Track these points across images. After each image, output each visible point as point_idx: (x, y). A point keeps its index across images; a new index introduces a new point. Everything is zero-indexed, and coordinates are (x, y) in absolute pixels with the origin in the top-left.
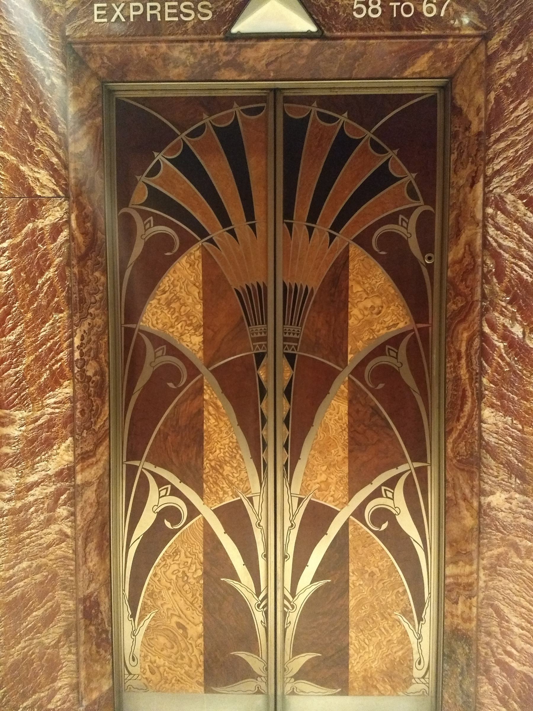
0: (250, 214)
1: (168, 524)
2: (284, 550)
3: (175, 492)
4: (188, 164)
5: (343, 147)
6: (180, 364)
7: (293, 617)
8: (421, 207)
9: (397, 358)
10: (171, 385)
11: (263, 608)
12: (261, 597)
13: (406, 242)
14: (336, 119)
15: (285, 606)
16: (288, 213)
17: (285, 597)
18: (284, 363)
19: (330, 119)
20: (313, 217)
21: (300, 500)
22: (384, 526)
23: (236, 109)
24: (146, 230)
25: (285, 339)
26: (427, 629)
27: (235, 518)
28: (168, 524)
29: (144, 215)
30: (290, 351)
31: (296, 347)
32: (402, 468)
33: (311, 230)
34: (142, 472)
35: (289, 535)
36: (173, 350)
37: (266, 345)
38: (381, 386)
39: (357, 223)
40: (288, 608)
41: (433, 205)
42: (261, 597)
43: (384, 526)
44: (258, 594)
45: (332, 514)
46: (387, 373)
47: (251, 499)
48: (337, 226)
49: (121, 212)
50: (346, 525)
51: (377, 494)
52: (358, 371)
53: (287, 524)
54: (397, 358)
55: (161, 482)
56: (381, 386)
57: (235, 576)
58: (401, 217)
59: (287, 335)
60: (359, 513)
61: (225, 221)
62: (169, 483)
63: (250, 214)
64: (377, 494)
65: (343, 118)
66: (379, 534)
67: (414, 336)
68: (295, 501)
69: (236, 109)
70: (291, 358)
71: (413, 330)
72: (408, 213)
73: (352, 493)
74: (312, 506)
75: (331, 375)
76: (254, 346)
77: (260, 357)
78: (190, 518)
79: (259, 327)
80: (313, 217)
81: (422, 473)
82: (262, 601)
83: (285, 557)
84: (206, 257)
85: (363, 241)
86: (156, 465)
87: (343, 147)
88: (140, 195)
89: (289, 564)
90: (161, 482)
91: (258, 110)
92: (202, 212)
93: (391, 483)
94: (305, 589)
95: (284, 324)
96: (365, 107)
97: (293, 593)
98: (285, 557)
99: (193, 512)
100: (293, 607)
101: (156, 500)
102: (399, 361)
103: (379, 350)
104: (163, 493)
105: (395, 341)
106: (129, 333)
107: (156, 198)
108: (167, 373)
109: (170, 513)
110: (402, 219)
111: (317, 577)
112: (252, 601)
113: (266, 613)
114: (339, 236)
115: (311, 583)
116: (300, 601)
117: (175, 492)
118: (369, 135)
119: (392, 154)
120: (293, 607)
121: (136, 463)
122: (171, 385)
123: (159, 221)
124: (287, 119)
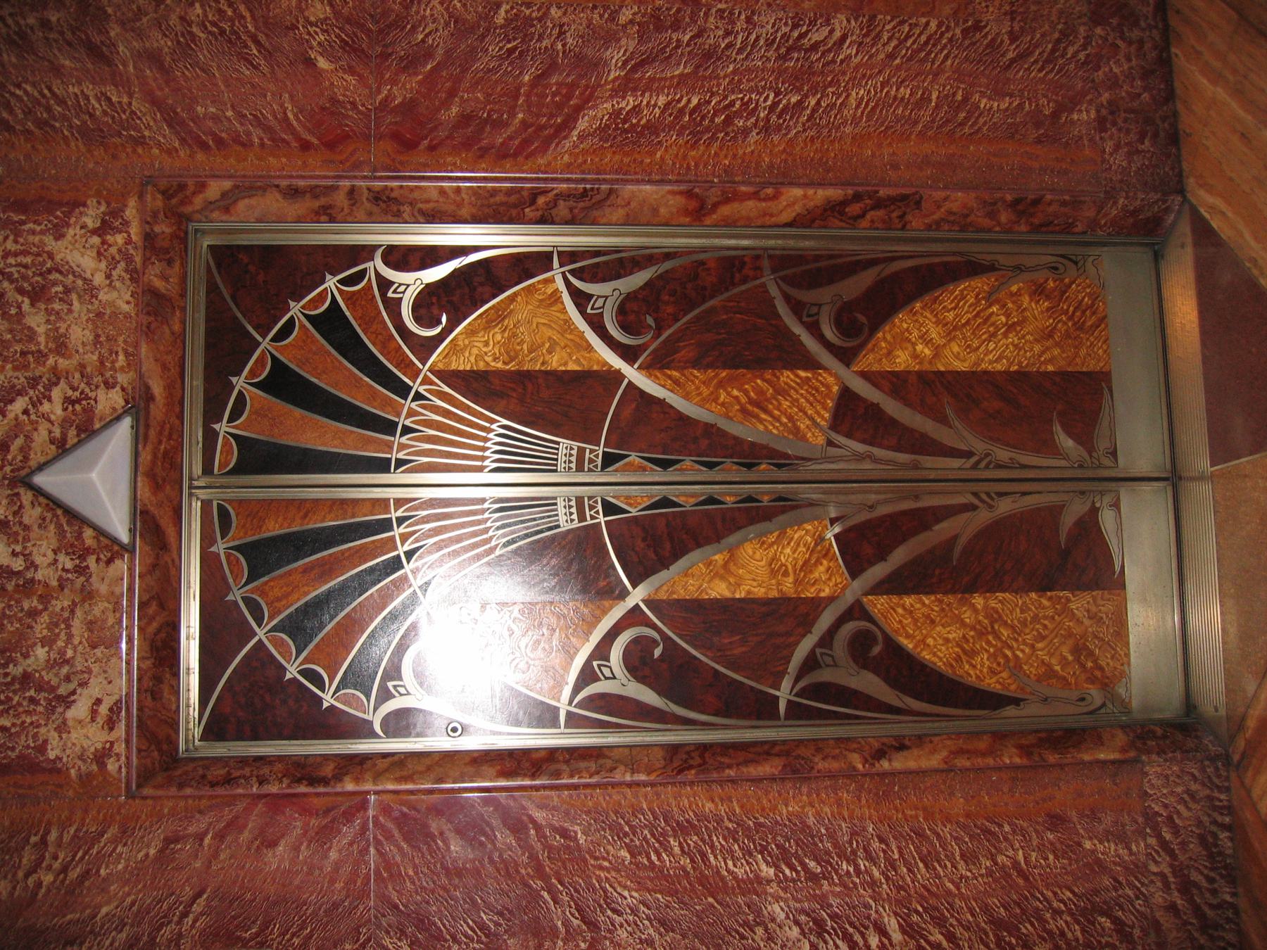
1: (876, 650)
2: (904, 466)
3: (827, 640)
5: (283, 383)
8: (378, 264)
9: (607, 297)
10: (657, 652)
11: (992, 499)
12: (976, 502)
14: (240, 393)
15: (987, 467)
17: (975, 467)
22: (862, 318)
23: (220, 547)
25: (580, 468)
28: (876, 650)
31: (592, 451)
32: (774, 291)
33: (407, 430)
34: (796, 695)
37: (590, 498)
40: (990, 463)
41: (374, 248)
42: (976, 502)
43: (862, 318)
44: (973, 508)
50: (864, 375)
52: (628, 354)
53: (867, 465)
54: (607, 297)
55: (811, 664)
58: (390, 294)
59: (573, 466)
60: (846, 356)
62: (813, 651)
64: (814, 329)
66: (874, 329)
67: (572, 272)
68: (832, 451)
69: (220, 547)
71: (563, 273)
72: (385, 284)
76: (592, 518)
79: (561, 510)
82: (983, 501)
87: (283, 383)
91: (224, 515)
93: (797, 308)
95: (556, 471)
96: (226, 350)
97: (968, 454)
99: (856, 611)
100: (987, 455)
109: (860, 647)
110: (395, 292)
111: (943, 420)
112: (983, 517)
113: (1000, 494)
115: (951, 427)
118: (265, 344)
119: (295, 309)
120: (987, 455)
121: (782, 706)
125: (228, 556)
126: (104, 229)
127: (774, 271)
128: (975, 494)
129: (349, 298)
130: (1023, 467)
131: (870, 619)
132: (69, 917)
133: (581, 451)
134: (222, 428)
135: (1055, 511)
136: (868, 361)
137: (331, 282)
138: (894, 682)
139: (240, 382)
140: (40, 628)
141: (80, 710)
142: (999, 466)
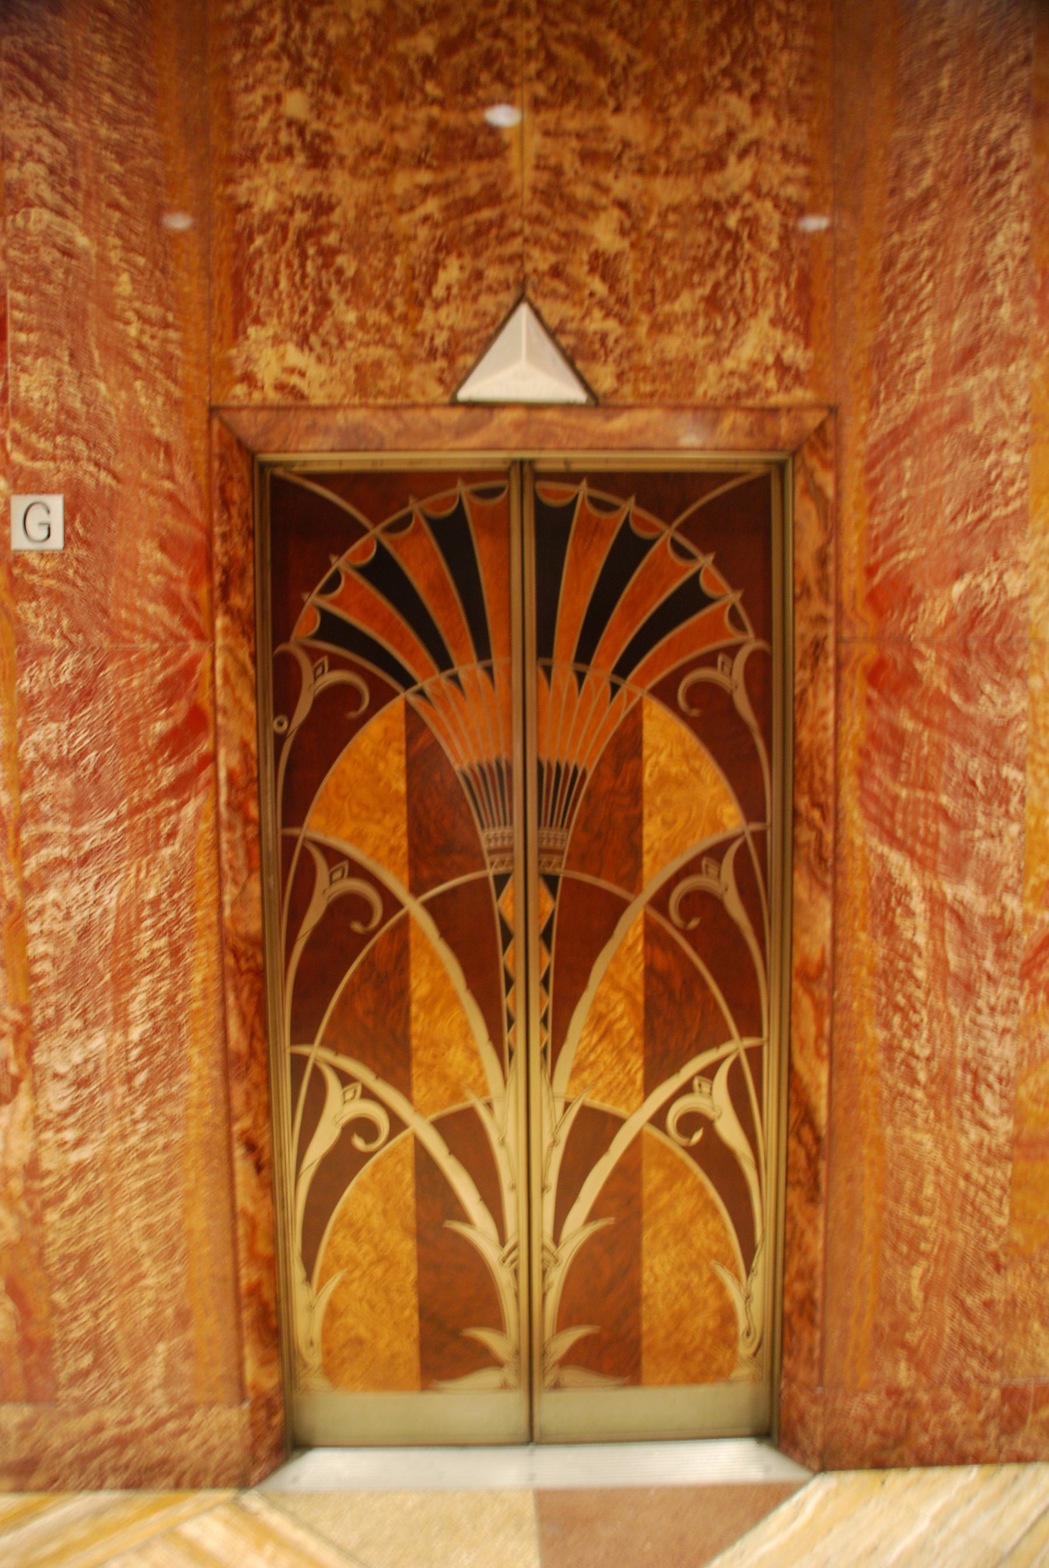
2: (543, 1177)
4: (384, 573)
5: (628, 551)
7: (557, 1277)
8: (751, 643)
10: (357, 927)
13: (729, 699)
16: (545, 647)
17: (543, 1248)
18: (539, 889)
19: (609, 508)
20: (585, 653)
21: (567, 1105)
22: (697, 1137)
23: (462, 489)
25: (541, 851)
26: (759, 1284)
27: (465, 1132)
29: (314, 655)
30: (549, 870)
32: (725, 1049)
35: (549, 1156)
36: (357, 870)
38: (694, 923)
43: (697, 1137)
44: (503, 1242)
45: (618, 1122)
46: (702, 903)
47: (489, 1105)
48: (623, 669)
49: (279, 649)
51: (687, 1089)
52: (659, 902)
53: (547, 1140)
55: (346, 1079)
56: (694, 923)
57: (466, 1219)
60: (658, 1119)
64: (687, 1089)
68: (560, 1106)
69: (462, 489)
70: (551, 881)
71: (742, 834)
72: (732, 651)
73: (648, 1089)
74: (586, 1111)
77: (501, 880)
78: (393, 1132)
79: (499, 831)
80: (585, 653)
81: (755, 1055)
83: (543, 1189)
84: (413, 720)
85: (665, 693)
86: (337, 1051)
87: (628, 551)
89: (550, 1197)
90: (346, 1079)
91: (494, 492)
93: (709, 1072)
94: (575, 1234)
96: (662, 489)
97: (556, 1239)
98: (543, 1189)
99: (397, 1124)
101: (340, 1108)
102: (723, 882)
103: (691, 868)
104: (349, 1095)
105: (717, 852)
106: (289, 843)
107: (333, 628)
108: (348, 907)
111: (593, 1216)
113: (516, 1272)
114: (627, 685)
116: (567, 1252)
117: (368, 1094)
118: (669, 533)
119: (705, 561)
120: (556, 1261)
122: (357, 927)
123: (336, 664)
125: (453, 498)
126: (781, 367)
127: (749, 1051)
128: (515, 1247)
129: (717, 615)
130: (544, 1295)
131: (391, 1136)
132: (96, 354)
133: (561, 853)
134: (583, 489)
135: (498, 1324)
137: (733, 597)
138: (327, 1162)
139: (629, 506)
140: (376, 316)
141: (294, 356)
142: (544, 1272)
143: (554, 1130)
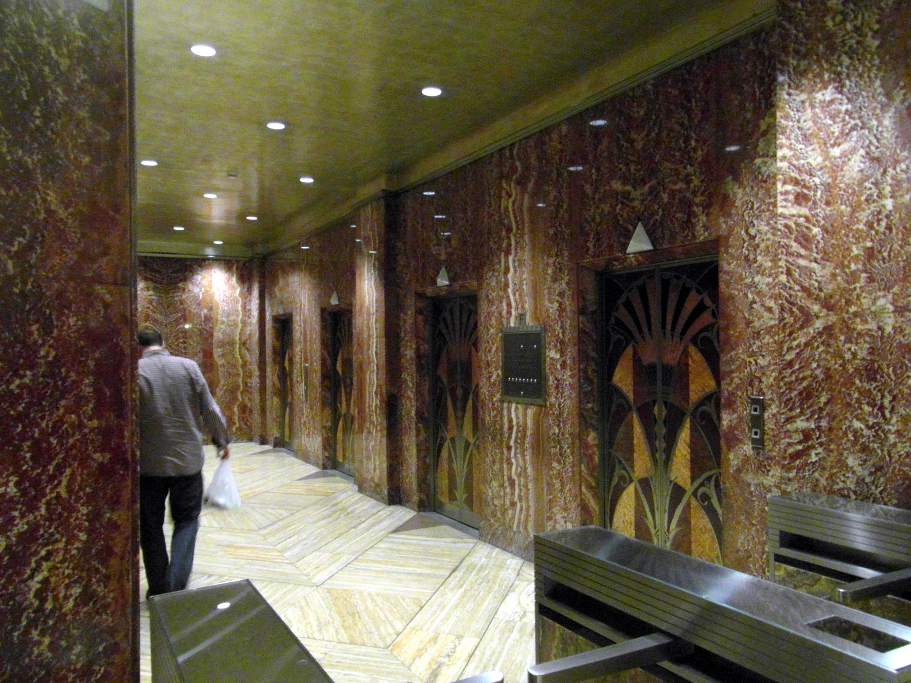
0: (650, 329)
4: (628, 305)
6: (626, 406)
22: (706, 503)
24: (615, 337)
39: (691, 332)
60: (695, 493)
61: (641, 332)
63: (650, 329)
65: (684, 277)
75: (683, 414)
77: (654, 402)
85: (694, 341)
88: (613, 320)
92: (633, 328)
93: (709, 479)
107: (619, 323)
116: (671, 536)
117: (624, 468)
123: (619, 333)
124: (662, 279)
136: (694, 503)
143: (668, 492)
